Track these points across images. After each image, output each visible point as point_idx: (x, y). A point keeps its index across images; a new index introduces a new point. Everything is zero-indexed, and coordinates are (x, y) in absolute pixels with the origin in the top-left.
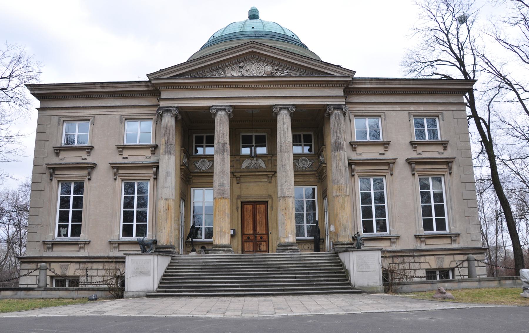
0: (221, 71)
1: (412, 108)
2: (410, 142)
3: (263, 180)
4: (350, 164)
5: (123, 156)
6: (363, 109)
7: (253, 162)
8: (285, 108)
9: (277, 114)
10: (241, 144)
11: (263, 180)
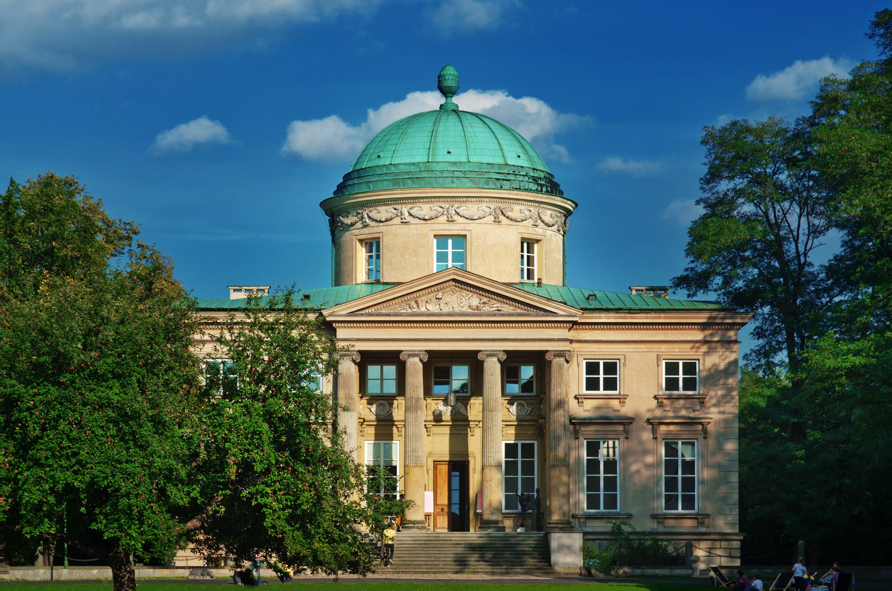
0: (413, 304)
1: (663, 347)
8: (493, 355)
9: (482, 362)
10: (433, 380)
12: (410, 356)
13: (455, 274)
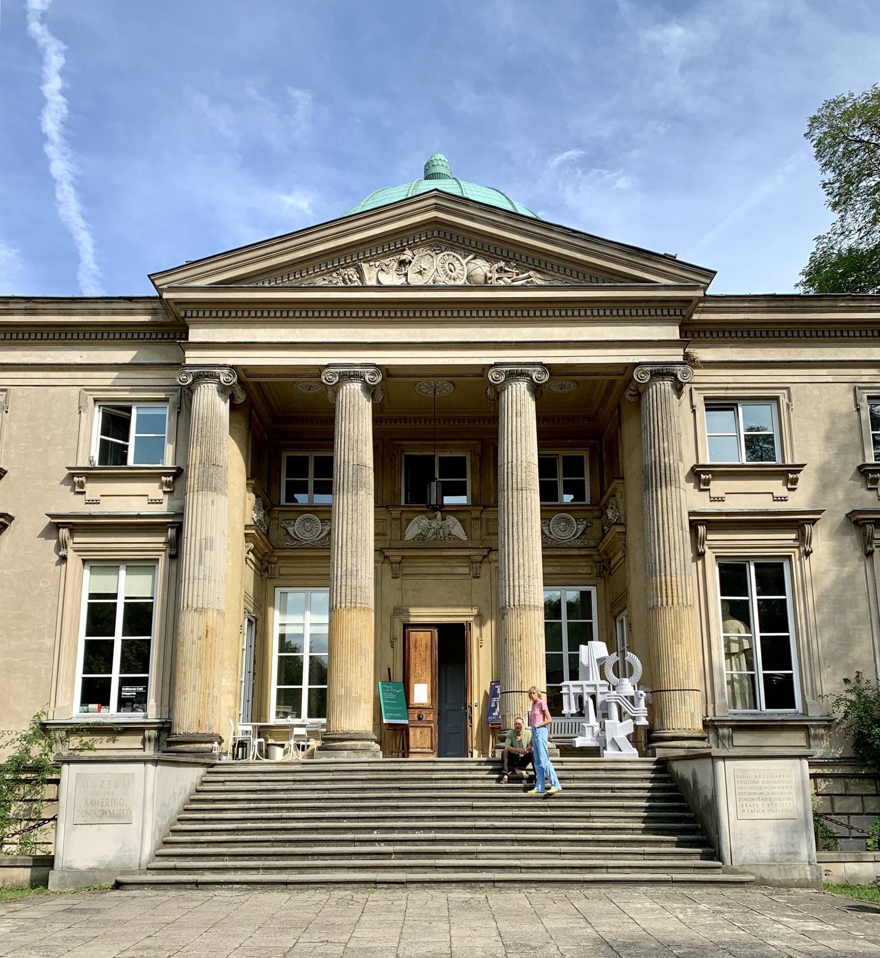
2: (859, 468)
3: (460, 570)
4: (693, 525)
5: (88, 496)
6: (730, 379)
7: (434, 524)
8: (522, 374)
9: (498, 392)
11: (460, 570)
12: (346, 377)
13: (438, 208)
